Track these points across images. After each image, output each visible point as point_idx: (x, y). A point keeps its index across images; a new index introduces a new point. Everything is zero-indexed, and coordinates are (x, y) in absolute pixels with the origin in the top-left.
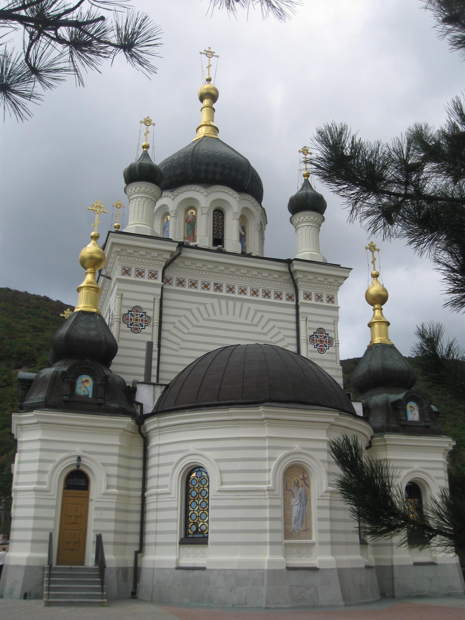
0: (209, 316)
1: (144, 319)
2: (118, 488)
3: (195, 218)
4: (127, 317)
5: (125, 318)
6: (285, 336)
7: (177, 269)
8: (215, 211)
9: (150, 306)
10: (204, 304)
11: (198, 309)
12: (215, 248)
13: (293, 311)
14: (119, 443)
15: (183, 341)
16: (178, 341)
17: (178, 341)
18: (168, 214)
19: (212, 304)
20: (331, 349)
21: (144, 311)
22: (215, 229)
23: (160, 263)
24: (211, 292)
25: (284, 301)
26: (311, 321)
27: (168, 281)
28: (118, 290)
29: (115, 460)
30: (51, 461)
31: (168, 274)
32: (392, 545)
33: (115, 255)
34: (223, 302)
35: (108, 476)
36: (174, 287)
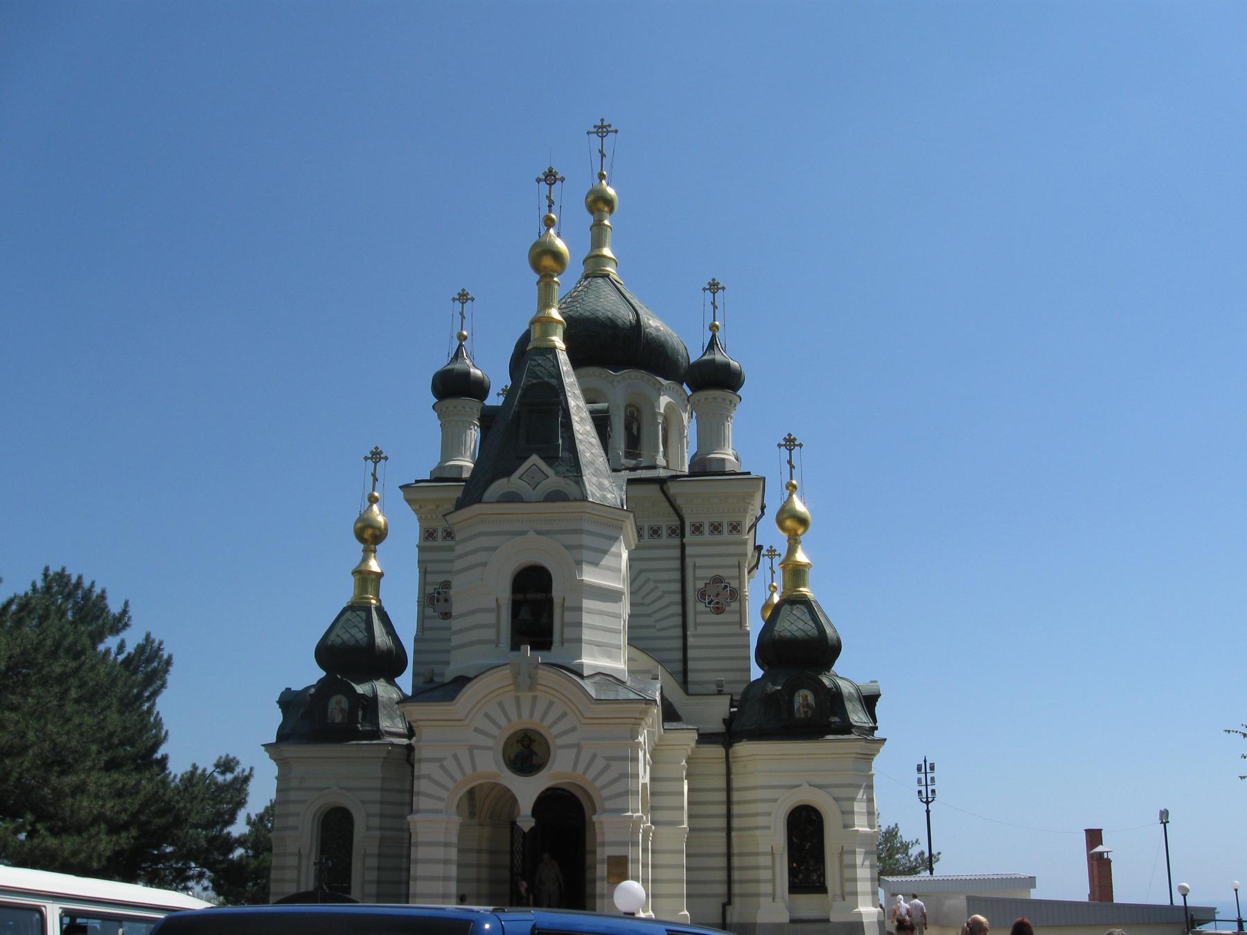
2: (381, 828)
6: (665, 593)
13: (676, 553)
20: (734, 606)
25: (665, 539)
26: (700, 567)
29: (377, 796)
32: (758, 895)
35: (368, 815)
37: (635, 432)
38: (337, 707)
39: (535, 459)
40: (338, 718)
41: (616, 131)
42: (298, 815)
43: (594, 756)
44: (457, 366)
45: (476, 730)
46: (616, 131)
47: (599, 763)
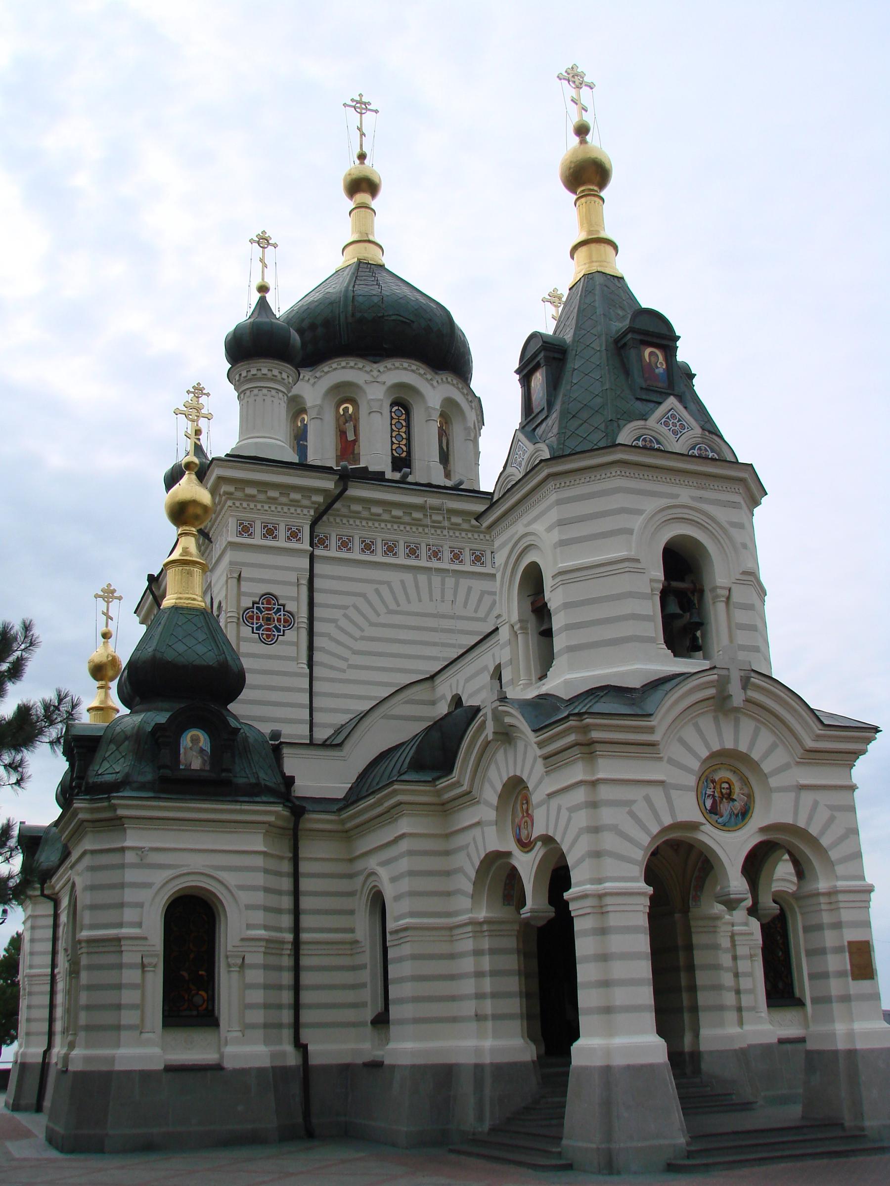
0: (399, 605)
1: (282, 617)
2: (266, 928)
3: (354, 419)
4: (251, 614)
5: (247, 617)
7: (338, 520)
8: (393, 404)
9: (292, 591)
10: (388, 584)
11: (377, 591)
12: (397, 476)
14: (262, 848)
15: (355, 652)
16: (346, 653)
17: (346, 653)
18: (304, 410)
19: (402, 582)
21: (281, 602)
22: (394, 439)
23: (305, 511)
24: (401, 560)
27: (322, 542)
28: (231, 563)
29: (259, 879)
30: (147, 885)
31: (320, 530)
33: (224, 498)
34: (422, 578)
36: (333, 553)
37: (445, 447)
38: (194, 747)
39: (672, 401)
40: (196, 764)
41: (376, 112)
42: (140, 905)
43: (816, 804)
44: (264, 319)
45: (671, 761)
46: (376, 112)
47: (822, 815)
